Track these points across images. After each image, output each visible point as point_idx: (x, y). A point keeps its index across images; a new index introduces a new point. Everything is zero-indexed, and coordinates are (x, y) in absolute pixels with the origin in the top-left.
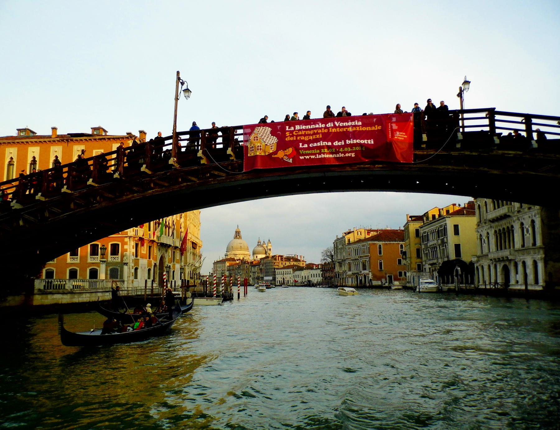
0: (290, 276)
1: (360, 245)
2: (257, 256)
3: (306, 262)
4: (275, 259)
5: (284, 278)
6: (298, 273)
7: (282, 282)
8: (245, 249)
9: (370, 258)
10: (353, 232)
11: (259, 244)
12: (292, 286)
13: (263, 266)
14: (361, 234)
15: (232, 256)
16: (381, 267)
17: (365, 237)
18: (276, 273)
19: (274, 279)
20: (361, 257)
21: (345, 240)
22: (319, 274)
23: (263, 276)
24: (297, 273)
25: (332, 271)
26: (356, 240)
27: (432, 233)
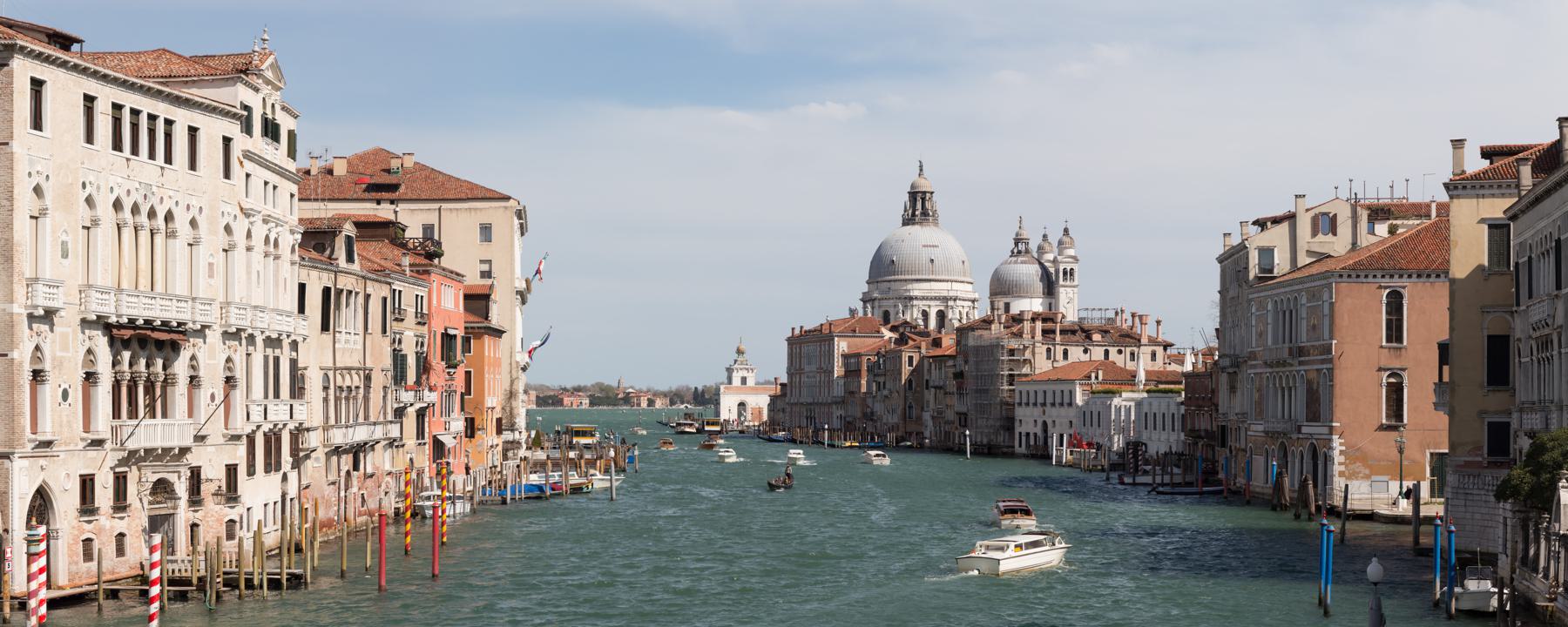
0: (1071, 413)
1: (1301, 290)
3: (1171, 345)
4: (1019, 335)
5: (1045, 423)
7: (1041, 442)
10: (1291, 217)
11: (1020, 246)
13: (966, 362)
14: (1333, 230)
17: (1354, 244)
18: (1017, 400)
19: (1009, 424)
20: (1301, 351)
21: (1247, 258)
22: (1173, 415)
27: (1543, 254)
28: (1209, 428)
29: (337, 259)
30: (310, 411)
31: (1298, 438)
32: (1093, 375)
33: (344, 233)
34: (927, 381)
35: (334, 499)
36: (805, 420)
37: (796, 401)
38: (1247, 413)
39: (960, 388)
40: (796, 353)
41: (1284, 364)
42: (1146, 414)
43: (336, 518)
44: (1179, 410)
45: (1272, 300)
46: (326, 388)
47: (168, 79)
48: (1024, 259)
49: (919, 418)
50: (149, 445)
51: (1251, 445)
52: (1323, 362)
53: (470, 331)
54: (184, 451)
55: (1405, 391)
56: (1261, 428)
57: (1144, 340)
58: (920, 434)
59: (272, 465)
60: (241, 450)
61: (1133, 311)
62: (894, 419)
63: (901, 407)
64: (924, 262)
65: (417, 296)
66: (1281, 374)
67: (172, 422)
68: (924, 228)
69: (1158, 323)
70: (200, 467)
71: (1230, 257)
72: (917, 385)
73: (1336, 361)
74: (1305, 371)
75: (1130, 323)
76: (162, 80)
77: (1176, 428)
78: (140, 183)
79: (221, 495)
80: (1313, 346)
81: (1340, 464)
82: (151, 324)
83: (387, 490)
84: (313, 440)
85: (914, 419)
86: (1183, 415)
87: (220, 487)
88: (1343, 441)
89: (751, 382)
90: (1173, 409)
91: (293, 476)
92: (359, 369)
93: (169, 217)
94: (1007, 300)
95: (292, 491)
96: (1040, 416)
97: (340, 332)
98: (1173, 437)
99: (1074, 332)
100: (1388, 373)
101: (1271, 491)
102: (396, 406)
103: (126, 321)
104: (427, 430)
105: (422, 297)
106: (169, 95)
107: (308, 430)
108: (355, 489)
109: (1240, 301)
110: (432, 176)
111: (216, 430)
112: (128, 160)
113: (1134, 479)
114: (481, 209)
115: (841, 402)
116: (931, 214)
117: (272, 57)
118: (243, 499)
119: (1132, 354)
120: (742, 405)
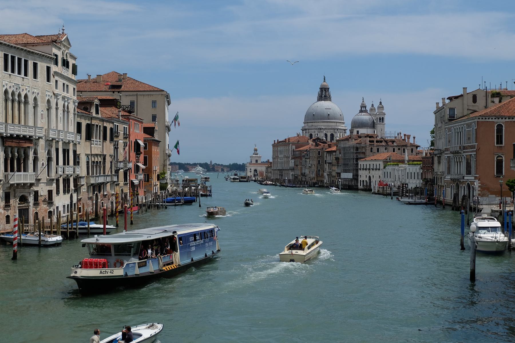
0: (380, 173)
1: (464, 124)
2: (358, 132)
5: (370, 177)
8: (335, 119)
9: (476, 151)
10: (462, 96)
11: (363, 109)
12: (375, 193)
15: (313, 131)
16: (499, 170)
18: (359, 168)
19: (356, 177)
20: (464, 148)
22: (418, 173)
23: (339, 171)
24: (389, 169)
28: (431, 178)
29: (92, 113)
30: (82, 170)
31: (463, 181)
33: (95, 103)
34: (326, 161)
35: (91, 204)
36: (279, 176)
37: (275, 169)
38: (444, 172)
39: (338, 163)
40: (275, 151)
42: (408, 173)
43: (92, 211)
44: (420, 171)
46: (88, 163)
47: (25, 45)
48: (364, 114)
49: (323, 175)
50: (18, 182)
52: (472, 152)
53: (147, 141)
54: (32, 185)
55: (504, 162)
56: (449, 177)
57: (408, 145)
58: (322, 181)
59: (66, 190)
60: (54, 185)
61: (405, 134)
62: (313, 176)
63: (315, 171)
64: (325, 115)
65: (124, 127)
66: (457, 156)
67: (28, 174)
68: (326, 101)
69: (414, 138)
70: (38, 191)
71: (439, 111)
72: (322, 162)
74: (465, 155)
75: (403, 138)
76: (24, 45)
77: (419, 178)
78: (15, 84)
79: (46, 201)
80: (468, 146)
81: (479, 191)
82: (19, 137)
83: (112, 201)
84: (83, 182)
85: (321, 175)
86: (421, 173)
87: (45, 198)
88: (480, 182)
89: (259, 162)
90: (418, 171)
91: (75, 196)
92: (100, 155)
93: (26, 96)
94: (358, 130)
95: (75, 200)
96: (368, 174)
97: (93, 141)
98: (418, 182)
99: (381, 142)
100: (497, 156)
101: (452, 201)
102: (116, 169)
103: (9, 135)
104: (128, 178)
105: (126, 128)
106: (26, 50)
107: (81, 177)
108: (99, 200)
109: (442, 127)
110: (134, 82)
111: (44, 176)
112: (10, 75)
114: (152, 95)
115: (293, 169)
116: (328, 96)
117: (66, 36)
118: (55, 203)
120: (256, 171)
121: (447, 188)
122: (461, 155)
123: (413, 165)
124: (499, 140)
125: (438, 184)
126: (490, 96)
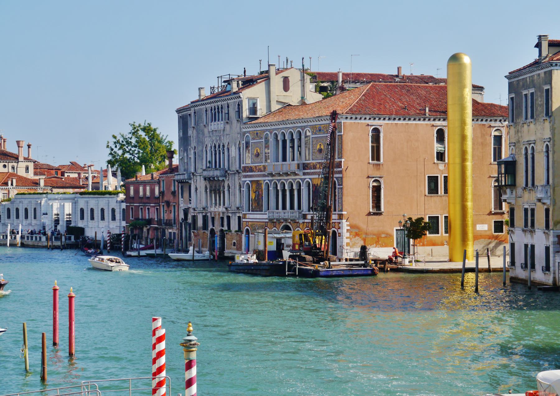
1: (305, 127)
6: (26, 202)
17: (303, 98)
21: (240, 105)
22: (113, 211)
25: (168, 204)
26: (275, 107)
32: (10, 183)
41: (295, 174)
42: (82, 211)
45: (271, 133)
51: (247, 227)
56: (266, 216)
57: (21, 159)
69: (29, 146)
73: (344, 172)
74: (310, 179)
81: (347, 238)
86: (124, 209)
88: (348, 223)
113: (139, 253)
119: (13, 168)
121: (250, 235)
122: (296, 179)
123: (96, 196)
124: (376, 155)
125: (210, 227)
126: (308, 81)
